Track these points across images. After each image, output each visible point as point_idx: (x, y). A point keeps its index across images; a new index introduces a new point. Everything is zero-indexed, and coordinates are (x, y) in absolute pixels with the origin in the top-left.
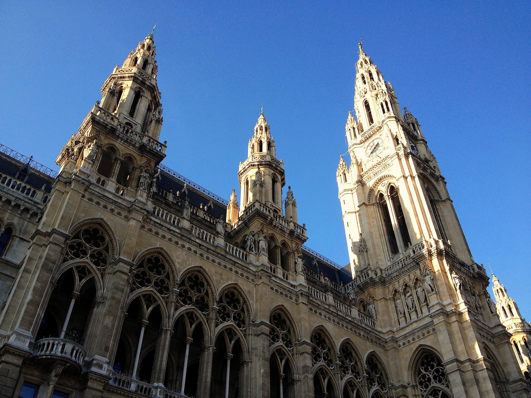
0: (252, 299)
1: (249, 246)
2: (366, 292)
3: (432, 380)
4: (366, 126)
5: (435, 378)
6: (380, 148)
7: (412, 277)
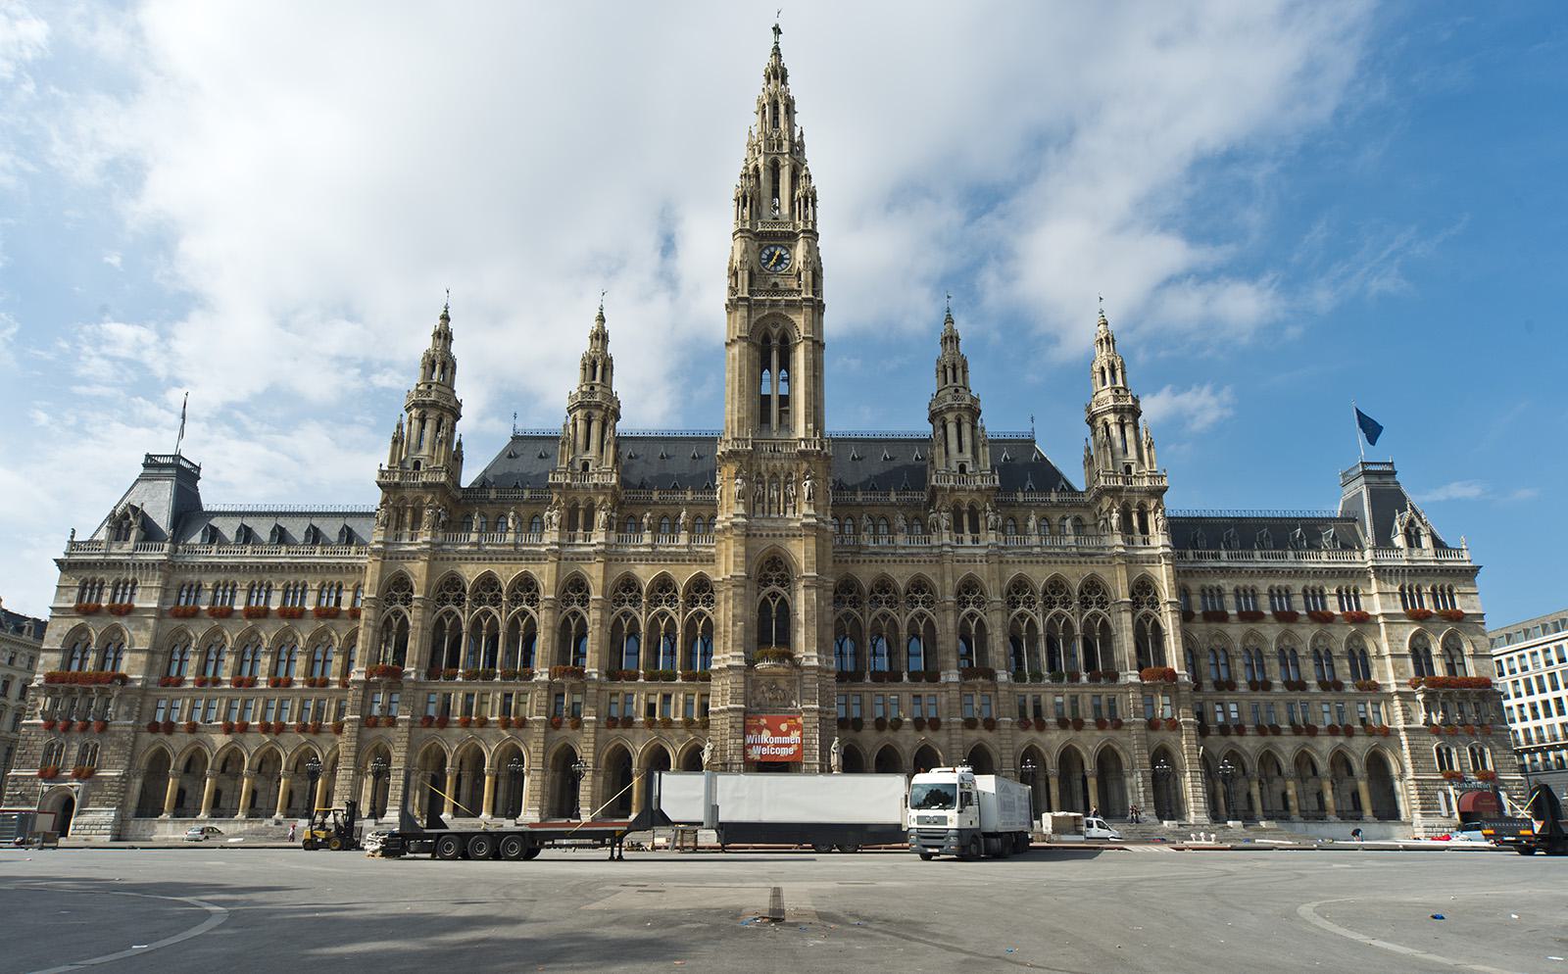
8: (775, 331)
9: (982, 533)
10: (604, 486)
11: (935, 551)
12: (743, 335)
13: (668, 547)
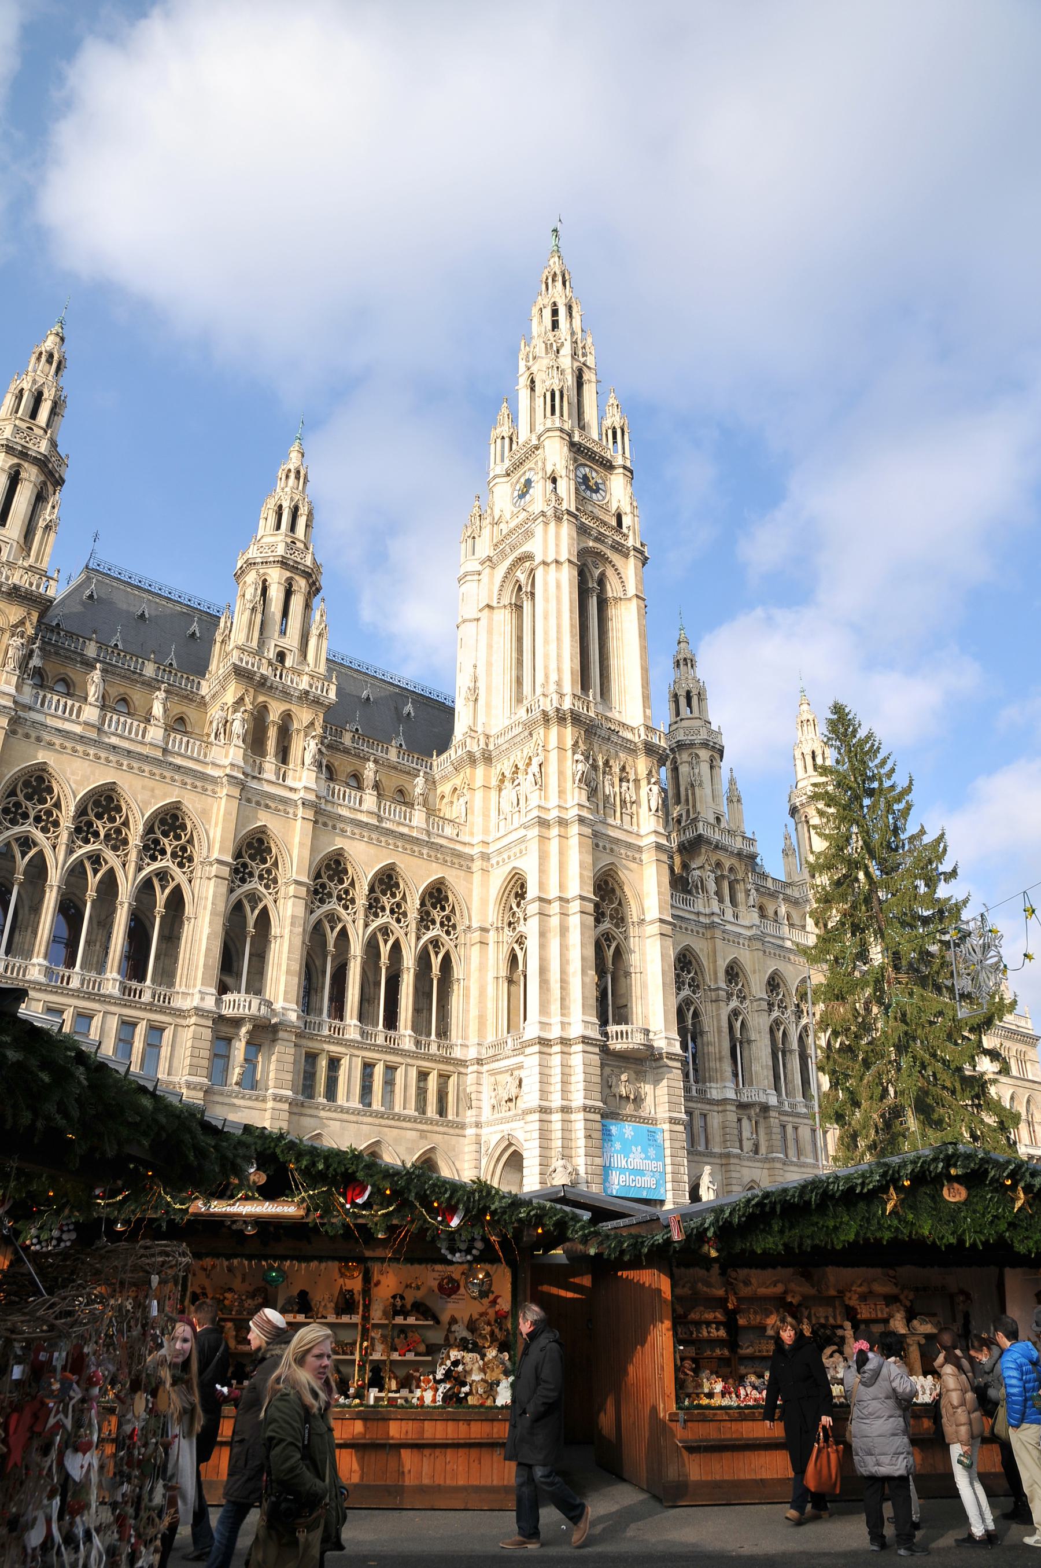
0: (209, 822)
7: (525, 753)
8: (597, 573)
9: (742, 908)
10: (316, 702)
11: (702, 919)
12: (572, 559)
13: (399, 824)
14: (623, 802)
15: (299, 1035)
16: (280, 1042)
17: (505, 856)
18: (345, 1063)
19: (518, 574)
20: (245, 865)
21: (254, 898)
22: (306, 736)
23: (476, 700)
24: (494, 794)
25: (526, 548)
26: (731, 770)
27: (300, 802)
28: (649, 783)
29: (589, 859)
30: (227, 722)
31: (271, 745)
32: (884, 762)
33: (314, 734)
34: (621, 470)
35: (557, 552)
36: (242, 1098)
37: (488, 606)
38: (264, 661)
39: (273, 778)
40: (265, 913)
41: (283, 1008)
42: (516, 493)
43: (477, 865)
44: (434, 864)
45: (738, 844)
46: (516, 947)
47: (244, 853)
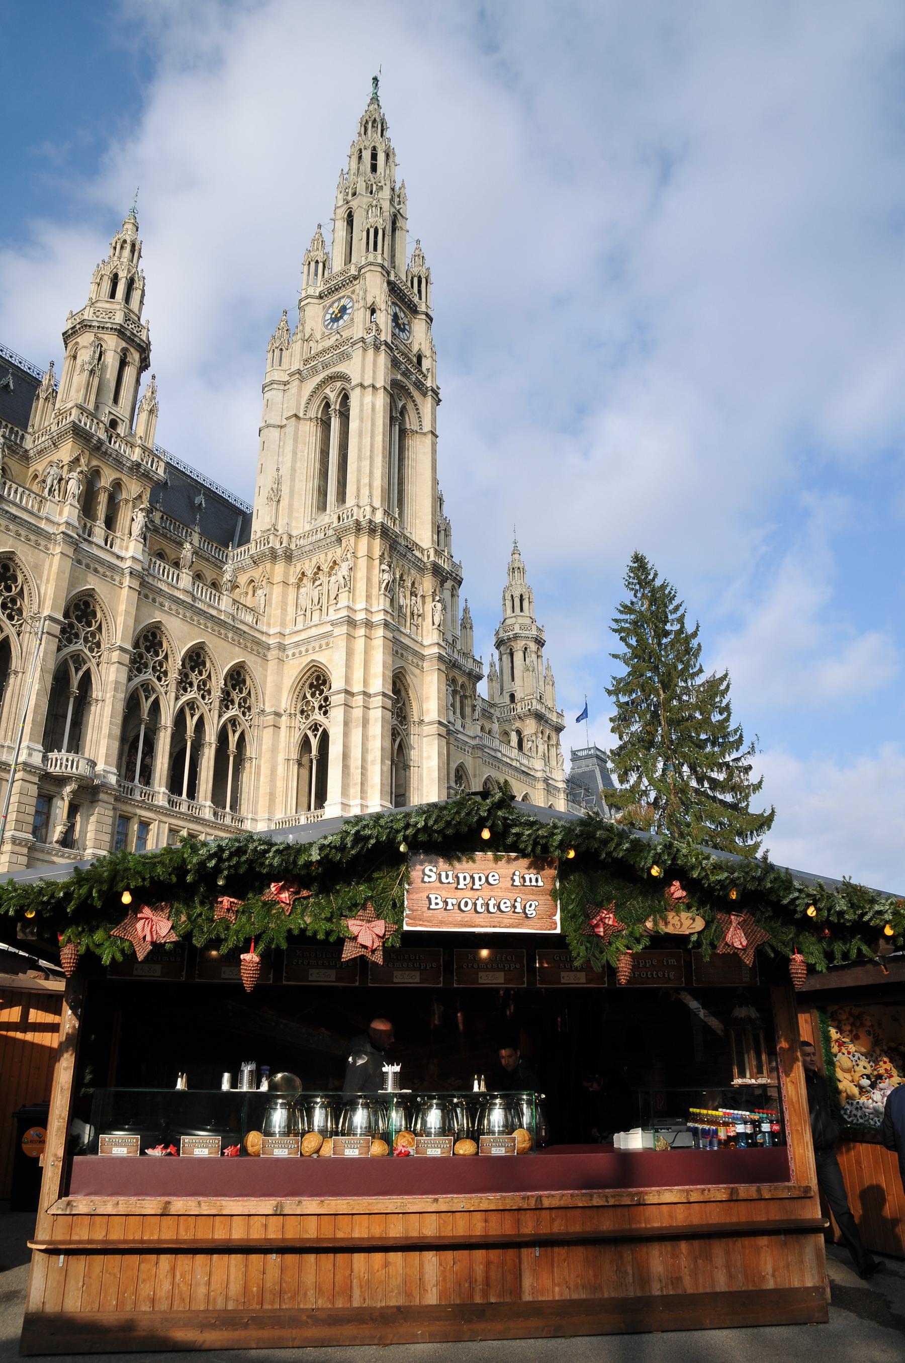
0: (41, 577)
1: (48, 487)
2: (261, 568)
3: (317, 710)
4: (337, 264)
5: (320, 707)
6: (346, 317)
8: (400, 404)
9: (468, 721)
13: (210, 606)
14: (412, 614)
15: (117, 799)
16: (100, 803)
17: (303, 649)
18: (153, 827)
19: (327, 391)
20: (71, 625)
21: (78, 660)
22: (134, 507)
23: (279, 501)
24: (292, 591)
25: (341, 368)
26: (466, 600)
27: (127, 571)
28: (433, 601)
29: (390, 660)
30: (61, 479)
31: (101, 511)
32: (677, 608)
33: (142, 506)
34: (424, 317)
35: (374, 378)
36: (62, 856)
37: (296, 416)
38: (101, 425)
39: (103, 544)
40: (87, 676)
41: (104, 771)
42: (328, 316)
43: (272, 654)
44: (237, 648)
45: (469, 665)
46: (310, 733)
47: (71, 614)
